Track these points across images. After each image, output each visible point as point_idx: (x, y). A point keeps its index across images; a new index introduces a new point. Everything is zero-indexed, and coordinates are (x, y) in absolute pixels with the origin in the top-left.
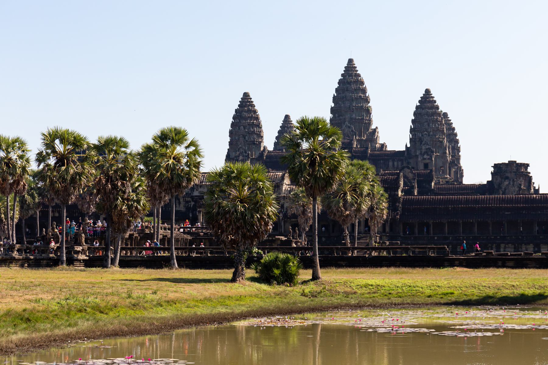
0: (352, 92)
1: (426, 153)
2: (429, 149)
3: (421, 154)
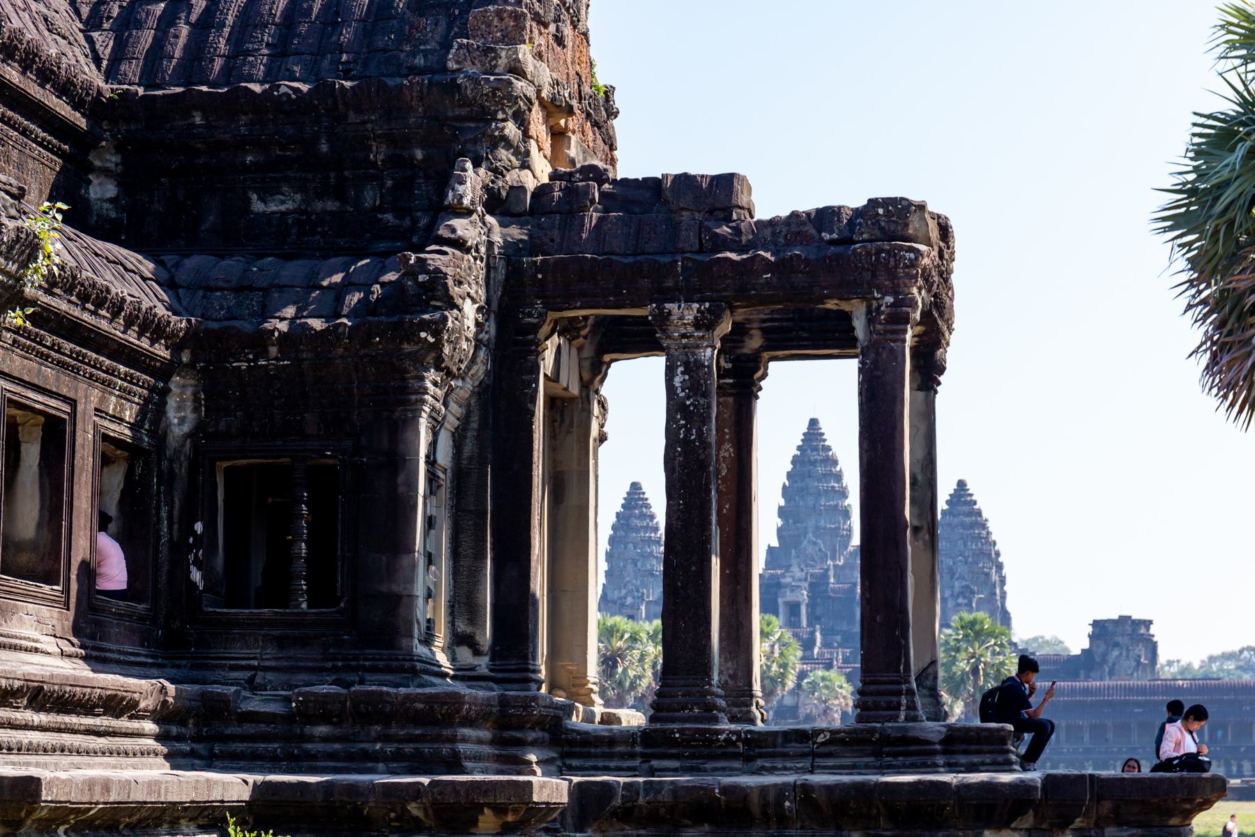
0: (819, 480)
1: (962, 594)
2: (967, 587)
3: (952, 595)
